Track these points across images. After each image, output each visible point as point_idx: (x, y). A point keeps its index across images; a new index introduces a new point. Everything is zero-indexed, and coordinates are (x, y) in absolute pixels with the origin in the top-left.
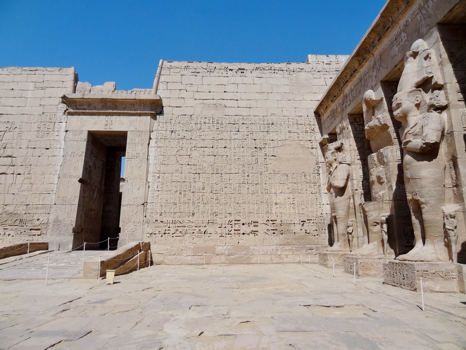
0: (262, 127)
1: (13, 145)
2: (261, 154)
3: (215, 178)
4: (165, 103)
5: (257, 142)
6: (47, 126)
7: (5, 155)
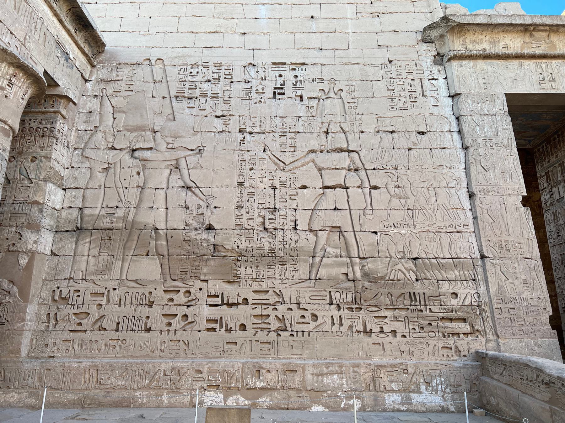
6: (406, 86)
7: (330, 148)
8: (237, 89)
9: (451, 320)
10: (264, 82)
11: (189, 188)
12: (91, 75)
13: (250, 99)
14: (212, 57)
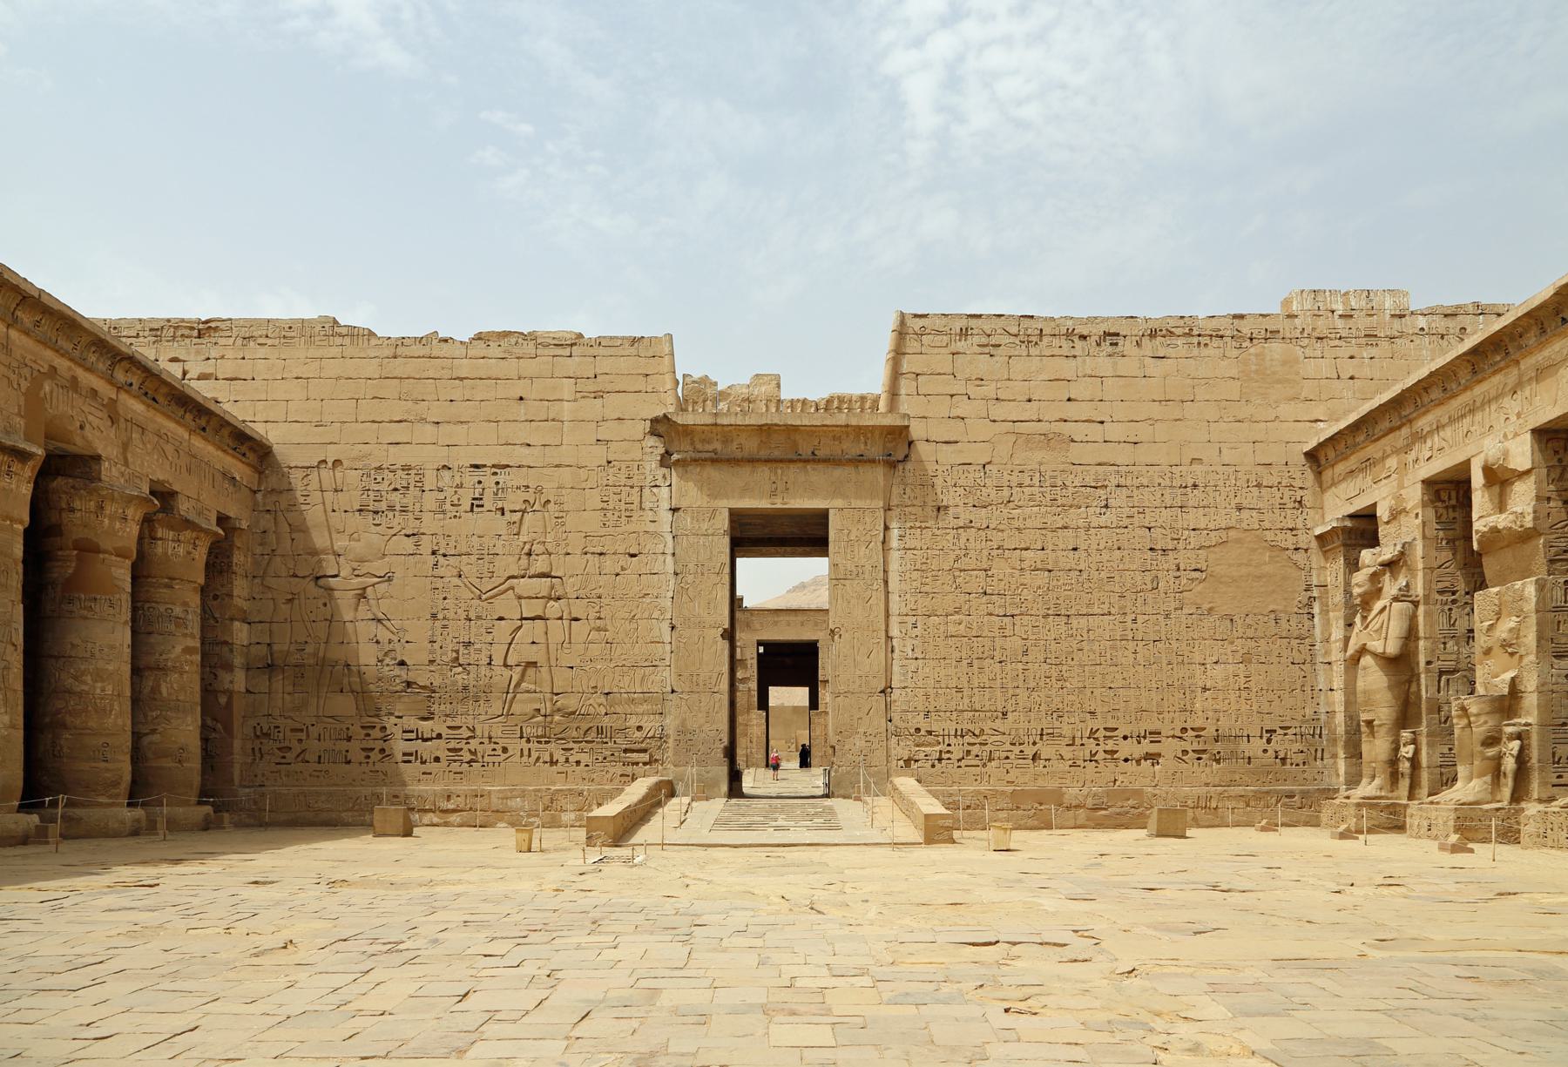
0: (1167, 496)
1: (549, 546)
2: (1166, 566)
3: (1057, 627)
4: (917, 431)
5: (1156, 533)
8: (430, 500)
9: (633, 751)
10: (460, 491)
11: (379, 621)
12: (259, 484)
13: (444, 512)
14: (400, 456)
